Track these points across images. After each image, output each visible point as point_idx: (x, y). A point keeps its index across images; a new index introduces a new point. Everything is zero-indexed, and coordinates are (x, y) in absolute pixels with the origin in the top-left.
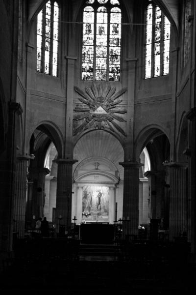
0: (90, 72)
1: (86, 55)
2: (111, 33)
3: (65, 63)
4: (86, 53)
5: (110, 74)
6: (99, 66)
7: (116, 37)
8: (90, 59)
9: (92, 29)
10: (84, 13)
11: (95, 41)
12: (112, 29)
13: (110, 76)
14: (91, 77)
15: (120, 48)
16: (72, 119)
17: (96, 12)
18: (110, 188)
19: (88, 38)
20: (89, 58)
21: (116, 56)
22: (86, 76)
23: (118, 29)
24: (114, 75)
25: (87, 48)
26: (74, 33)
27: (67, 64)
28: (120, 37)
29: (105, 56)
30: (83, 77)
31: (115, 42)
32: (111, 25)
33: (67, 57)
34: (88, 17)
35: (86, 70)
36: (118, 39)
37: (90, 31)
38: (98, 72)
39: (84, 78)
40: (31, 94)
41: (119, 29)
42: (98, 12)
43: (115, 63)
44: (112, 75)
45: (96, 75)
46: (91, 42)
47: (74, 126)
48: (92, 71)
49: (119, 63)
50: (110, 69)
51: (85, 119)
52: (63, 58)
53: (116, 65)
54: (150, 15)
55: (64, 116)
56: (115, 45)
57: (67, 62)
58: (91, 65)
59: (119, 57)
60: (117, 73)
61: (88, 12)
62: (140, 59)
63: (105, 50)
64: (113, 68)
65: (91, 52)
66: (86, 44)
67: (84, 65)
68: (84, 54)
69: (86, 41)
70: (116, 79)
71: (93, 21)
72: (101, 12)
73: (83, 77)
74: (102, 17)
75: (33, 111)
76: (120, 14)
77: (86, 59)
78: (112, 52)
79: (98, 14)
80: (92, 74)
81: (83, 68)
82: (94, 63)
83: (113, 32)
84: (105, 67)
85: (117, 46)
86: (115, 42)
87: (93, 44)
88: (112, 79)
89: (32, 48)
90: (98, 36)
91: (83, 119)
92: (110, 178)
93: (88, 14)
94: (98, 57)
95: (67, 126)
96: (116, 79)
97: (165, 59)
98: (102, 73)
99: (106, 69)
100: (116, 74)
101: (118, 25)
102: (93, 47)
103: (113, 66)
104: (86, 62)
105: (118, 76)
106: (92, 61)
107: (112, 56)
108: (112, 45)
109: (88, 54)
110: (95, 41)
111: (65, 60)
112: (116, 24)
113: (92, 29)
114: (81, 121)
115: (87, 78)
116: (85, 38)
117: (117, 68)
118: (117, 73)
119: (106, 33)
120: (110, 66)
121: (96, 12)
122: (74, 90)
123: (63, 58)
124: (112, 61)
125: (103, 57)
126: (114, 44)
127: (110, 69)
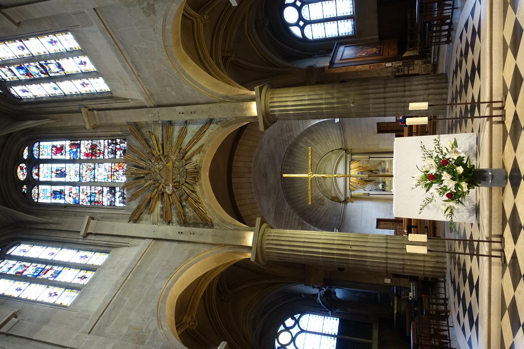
0: (115, 193)
1: (92, 199)
2: (63, 157)
3: (93, 238)
4: (89, 199)
5: (118, 157)
6: (106, 177)
7: (68, 149)
8: (97, 192)
9: (58, 188)
10: (40, 201)
11: (73, 184)
12: (59, 157)
13: (121, 156)
14: (122, 190)
15: (82, 142)
16: (183, 229)
17: (38, 183)
18: (352, 160)
19: (70, 196)
20: (95, 193)
21: (93, 147)
22: (121, 199)
23: (59, 146)
24: (118, 149)
25: (82, 196)
26: (56, 219)
27: (96, 234)
28: (68, 142)
29: (92, 166)
30: (122, 205)
31: (75, 150)
32: (54, 157)
33: (82, 233)
34: (43, 195)
35: (113, 199)
36: (71, 145)
37: (61, 192)
38: (115, 178)
39: (123, 203)
40: (89, 333)
41: (58, 144)
42: (38, 179)
43: (102, 148)
44: (118, 153)
45: (119, 181)
46: (75, 190)
47: (196, 225)
48: (114, 188)
49: (102, 141)
50: (111, 156)
51: (184, 203)
52: (85, 241)
53: (104, 147)
54: (24, 91)
55: (176, 244)
56: (79, 151)
57: (91, 234)
58: (106, 190)
59: (95, 142)
60: (116, 144)
61: (38, 194)
62: (84, 103)
63: (85, 165)
64: (108, 152)
65: (87, 189)
66: (77, 199)
67: (106, 203)
68: (90, 201)
69: (74, 199)
70: (124, 145)
71: (48, 187)
72: (38, 174)
73: (122, 205)
74: (45, 172)
75: (125, 330)
76: (41, 143)
77: (96, 199)
78: (87, 155)
79: (41, 179)
80: (117, 189)
81: (110, 205)
82: (101, 184)
83: (62, 154)
84: (108, 165)
85: (79, 146)
86: (75, 150)
87: (77, 188)
88: (124, 152)
89: (15, 315)
90: (67, 179)
91: (183, 207)
92: (340, 160)
93: (41, 195)
94: (94, 178)
95: (193, 238)
96: (124, 145)
97: (52, 49)
98: (117, 171)
99: (110, 164)
100: (118, 146)
101: (53, 146)
102: (81, 187)
103: (106, 151)
104: (101, 200)
105: (121, 142)
106: (100, 188)
107: (92, 155)
108: (78, 154)
109: (90, 196)
110: (73, 184)
111: (89, 237)
112: (52, 150)
113: (58, 188)
114: (187, 210)
115: (124, 198)
116: (69, 200)
117: (109, 145)
118: (116, 144)
119: (63, 165)
120: (107, 157)
121: (38, 183)
122: (135, 222)
123: (85, 241)
124: (100, 153)
125: (94, 169)
126: (77, 151)
127: (111, 156)
